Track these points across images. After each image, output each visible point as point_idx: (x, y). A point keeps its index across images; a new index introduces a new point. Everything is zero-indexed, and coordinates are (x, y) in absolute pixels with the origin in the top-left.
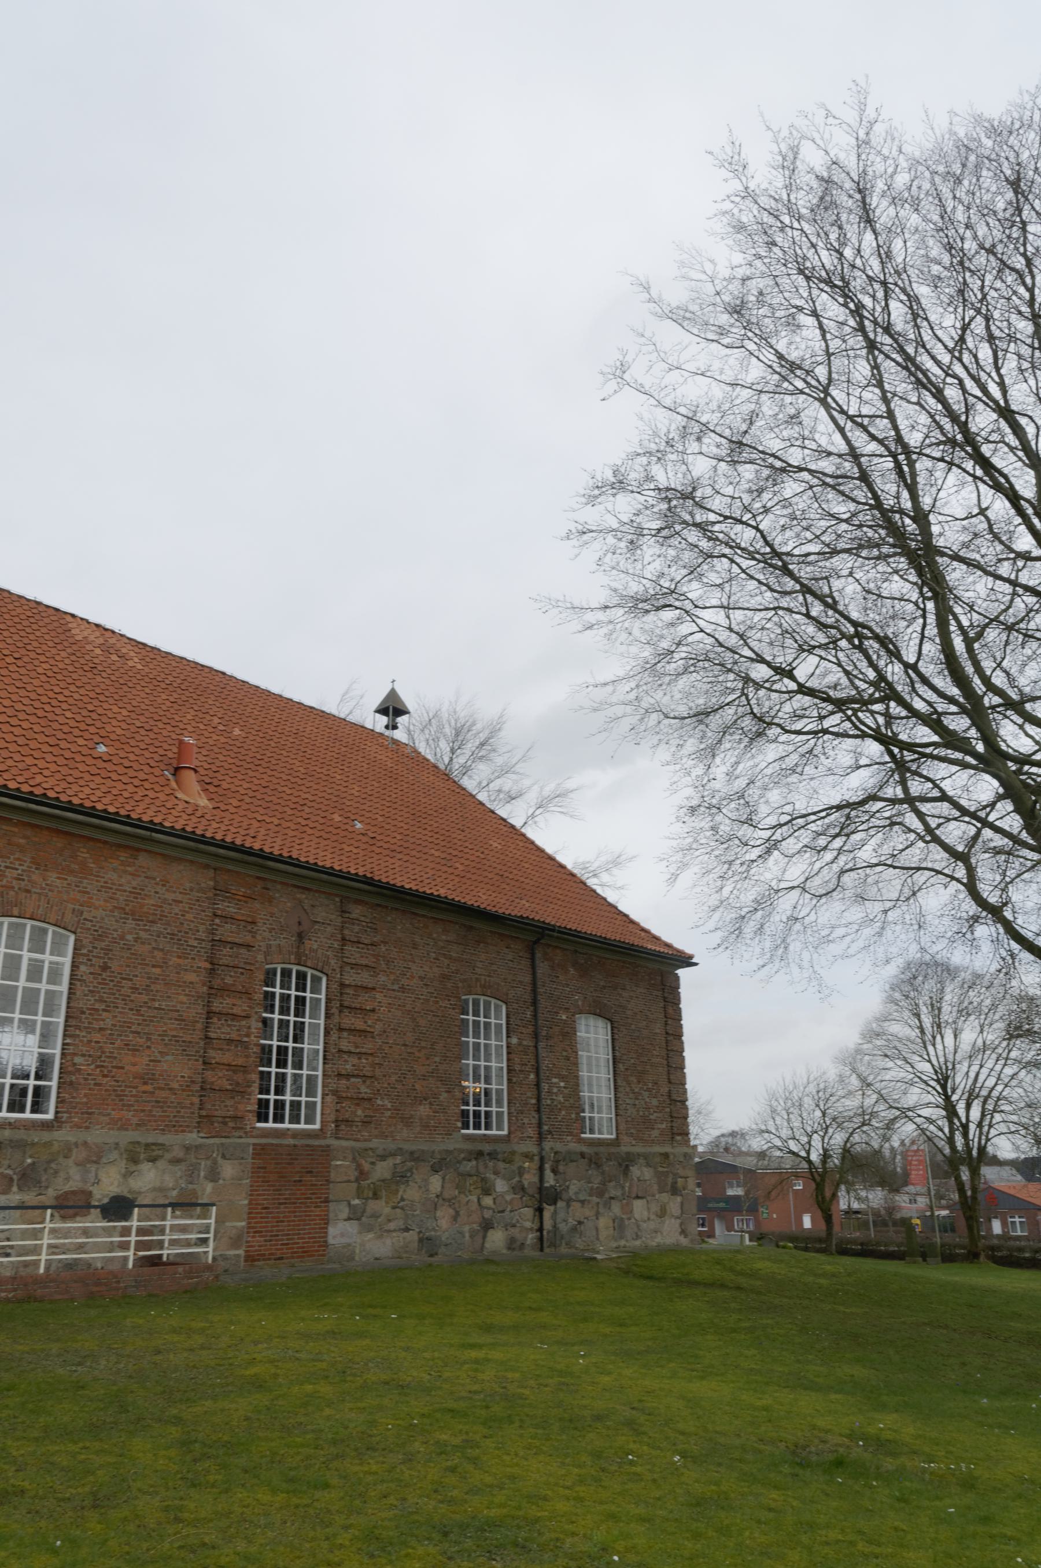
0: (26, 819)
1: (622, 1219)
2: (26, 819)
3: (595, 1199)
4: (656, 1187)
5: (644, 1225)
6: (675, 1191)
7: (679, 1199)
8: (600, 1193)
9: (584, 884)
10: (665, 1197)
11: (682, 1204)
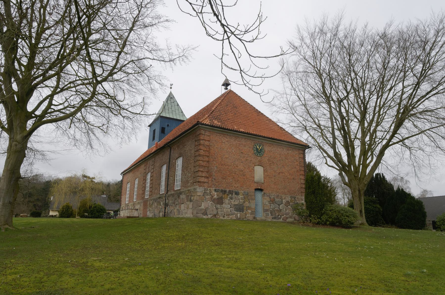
0: (271, 143)
1: (179, 210)
2: (271, 143)
3: (173, 205)
4: (186, 200)
5: (183, 211)
6: (191, 201)
7: (192, 203)
8: (174, 203)
9: (284, 130)
10: (188, 203)
11: (193, 204)
